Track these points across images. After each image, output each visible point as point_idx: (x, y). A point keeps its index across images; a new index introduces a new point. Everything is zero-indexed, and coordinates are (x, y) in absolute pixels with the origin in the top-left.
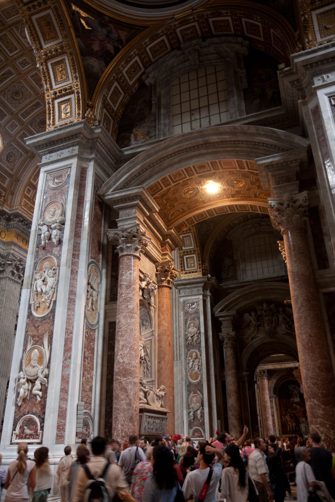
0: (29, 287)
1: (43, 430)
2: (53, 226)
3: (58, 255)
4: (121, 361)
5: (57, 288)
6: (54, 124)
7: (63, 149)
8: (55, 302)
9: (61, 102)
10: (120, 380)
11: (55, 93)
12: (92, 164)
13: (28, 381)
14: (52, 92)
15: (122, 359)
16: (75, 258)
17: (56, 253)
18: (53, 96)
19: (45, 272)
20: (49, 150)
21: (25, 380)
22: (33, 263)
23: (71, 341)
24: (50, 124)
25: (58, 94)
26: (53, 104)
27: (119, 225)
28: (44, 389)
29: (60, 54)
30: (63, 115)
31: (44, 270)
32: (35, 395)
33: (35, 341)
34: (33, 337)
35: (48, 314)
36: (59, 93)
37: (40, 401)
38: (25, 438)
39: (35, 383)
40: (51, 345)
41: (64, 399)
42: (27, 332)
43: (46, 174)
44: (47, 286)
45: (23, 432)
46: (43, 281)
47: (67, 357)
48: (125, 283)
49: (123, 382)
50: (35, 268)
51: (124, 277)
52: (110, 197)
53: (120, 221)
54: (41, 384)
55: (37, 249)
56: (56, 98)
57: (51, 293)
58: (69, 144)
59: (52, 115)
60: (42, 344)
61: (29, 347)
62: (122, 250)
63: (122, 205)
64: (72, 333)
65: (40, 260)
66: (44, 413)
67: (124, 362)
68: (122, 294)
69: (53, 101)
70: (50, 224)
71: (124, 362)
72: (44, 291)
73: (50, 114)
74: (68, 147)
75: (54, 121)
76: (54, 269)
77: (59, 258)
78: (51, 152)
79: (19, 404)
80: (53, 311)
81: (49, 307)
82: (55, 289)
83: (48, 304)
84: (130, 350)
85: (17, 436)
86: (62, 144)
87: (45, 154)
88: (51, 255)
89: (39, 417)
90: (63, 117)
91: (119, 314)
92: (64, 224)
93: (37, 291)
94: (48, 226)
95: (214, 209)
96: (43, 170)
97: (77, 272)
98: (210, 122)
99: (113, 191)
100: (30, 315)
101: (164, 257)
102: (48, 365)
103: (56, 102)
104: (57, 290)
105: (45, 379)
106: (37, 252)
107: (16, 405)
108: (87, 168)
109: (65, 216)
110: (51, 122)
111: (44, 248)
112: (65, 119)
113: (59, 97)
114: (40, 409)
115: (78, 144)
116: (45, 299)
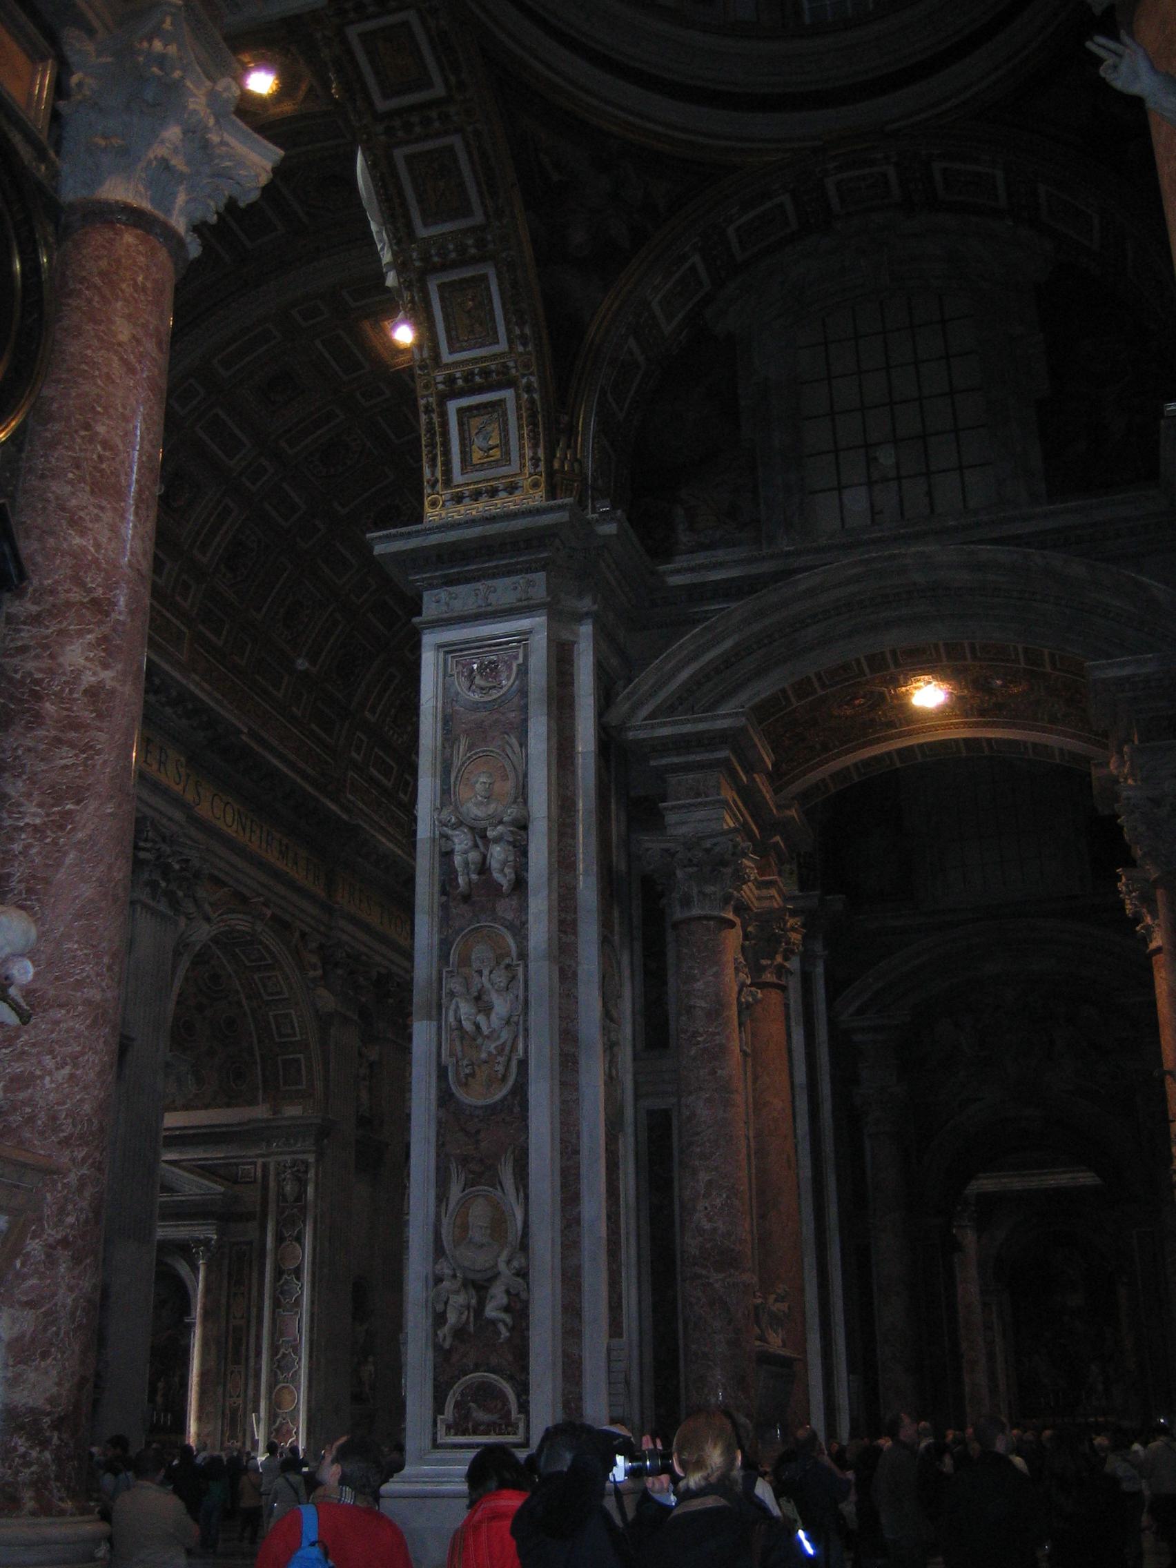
0: (434, 1012)
1: (527, 1413)
2: (491, 834)
3: (517, 923)
4: (707, 1226)
5: (526, 1021)
6: (448, 483)
7: (494, 576)
8: (523, 1064)
9: (470, 409)
10: (708, 1278)
11: (451, 380)
12: (586, 630)
13: (468, 1283)
14: (440, 376)
15: (710, 1220)
16: (565, 933)
17: (509, 916)
18: (441, 387)
19: (480, 972)
20: (445, 576)
21: (457, 1284)
22: (436, 939)
23: (578, 1175)
24: (437, 481)
25: (460, 382)
26: (443, 415)
27: (671, 818)
28: (519, 1309)
29: (475, 260)
30: (477, 456)
31: (476, 965)
32: (493, 1322)
33: (471, 1172)
34: (464, 1160)
35: (505, 1098)
36: (466, 379)
37: (509, 1340)
38: (475, 1433)
39: (486, 1288)
40: (526, 1187)
41: (571, 1330)
42: (441, 1146)
43: (441, 655)
44: (493, 1016)
45: (467, 1417)
46: (478, 999)
47: (571, 1223)
48: (703, 1005)
49: (717, 1286)
50: (444, 957)
51: (699, 985)
52: (642, 735)
53: (673, 807)
54: (508, 1292)
55: (444, 898)
56: (454, 393)
57: (505, 1035)
58: (518, 563)
59: (439, 450)
60: (495, 1182)
61: (455, 1192)
62: (686, 902)
63: (676, 760)
64: (577, 1152)
65: (457, 933)
66: (525, 1369)
67: (715, 1230)
68: (695, 1034)
69: (442, 404)
70: (482, 824)
71: (715, 1230)
72: (486, 1031)
73: (432, 445)
74: (509, 572)
75: (447, 472)
76: (508, 967)
77: (519, 930)
78: (450, 582)
79: (447, 1345)
80: (521, 1090)
81: (504, 1078)
82: (519, 1022)
83: (500, 1068)
84: (728, 1197)
85: (449, 1428)
86: (494, 564)
87: (432, 587)
88: (495, 920)
89: (510, 1378)
90: (475, 461)
91: (690, 1093)
92: (524, 827)
93: (460, 1027)
94: (472, 829)
95: (921, 746)
96: (429, 639)
97: (575, 974)
98: (929, 494)
99: (651, 716)
100: (445, 1098)
101: (765, 892)
102: (521, 1243)
103: (453, 406)
104: (526, 1030)
105: (520, 1280)
106: (444, 907)
107: (437, 1348)
108: (574, 643)
109: (525, 802)
110: (439, 475)
111: (466, 898)
112: (481, 467)
113: (461, 393)
114: (510, 1358)
115: (543, 568)
116: (490, 1053)
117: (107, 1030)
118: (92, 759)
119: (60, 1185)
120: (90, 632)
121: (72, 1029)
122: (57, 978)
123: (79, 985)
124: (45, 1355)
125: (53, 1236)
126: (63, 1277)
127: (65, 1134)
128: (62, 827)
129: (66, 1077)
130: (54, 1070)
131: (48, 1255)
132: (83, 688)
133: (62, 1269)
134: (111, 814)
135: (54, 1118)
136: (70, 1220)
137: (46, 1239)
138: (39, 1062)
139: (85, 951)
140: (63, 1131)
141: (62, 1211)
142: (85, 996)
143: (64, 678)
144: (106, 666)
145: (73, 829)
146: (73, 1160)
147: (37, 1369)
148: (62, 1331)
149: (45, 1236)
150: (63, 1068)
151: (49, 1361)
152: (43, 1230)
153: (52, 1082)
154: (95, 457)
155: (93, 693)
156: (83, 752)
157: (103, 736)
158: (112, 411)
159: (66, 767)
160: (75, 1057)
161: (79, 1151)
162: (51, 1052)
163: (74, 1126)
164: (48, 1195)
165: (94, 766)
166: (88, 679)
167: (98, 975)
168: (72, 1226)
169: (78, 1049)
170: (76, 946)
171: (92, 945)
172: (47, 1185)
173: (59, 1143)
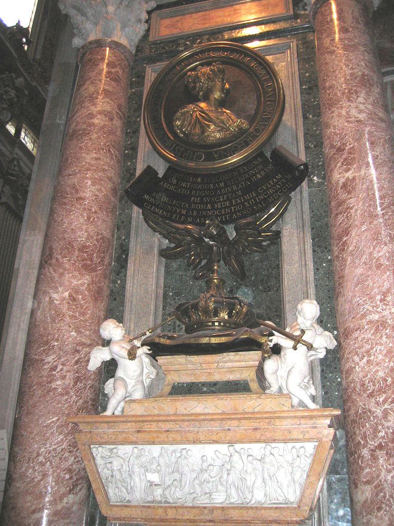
117: (388, 331)
118: (350, 212)
119: (372, 418)
120: (339, 162)
121: (364, 338)
122: (353, 318)
123: (364, 316)
124: (379, 509)
125: (372, 445)
126: (382, 466)
127: (370, 391)
128: (343, 250)
129: (366, 362)
130: (359, 362)
131: (372, 455)
132: (340, 186)
133: (381, 461)
134: (365, 230)
135: (363, 385)
136: (382, 434)
137: (370, 447)
138: (353, 361)
139: (364, 299)
140: (369, 390)
141: (376, 431)
142: (367, 320)
143: (334, 188)
144: (347, 170)
145: (347, 248)
146: (377, 403)
147: (376, 517)
148: (387, 495)
149: (369, 446)
150: (363, 359)
151: (382, 511)
152: (367, 442)
153: (359, 367)
154: (327, 96)
155: (345, 186)
156: (345, 213)
157: (352, 200)
158: (329, 74)
159: (341, 223)
160: (368, 352)
161: (380, 398)
162: (356, 353)
163: (374, 385)
164: (367, 424)
165: (351, 216)
166: (342, 181)
167: (373, 307)
168: (383, 438)
169: (369, 347)
170: (359, 299)
171: (367, 295)
172: (366, 419)
173: (368, 396)
